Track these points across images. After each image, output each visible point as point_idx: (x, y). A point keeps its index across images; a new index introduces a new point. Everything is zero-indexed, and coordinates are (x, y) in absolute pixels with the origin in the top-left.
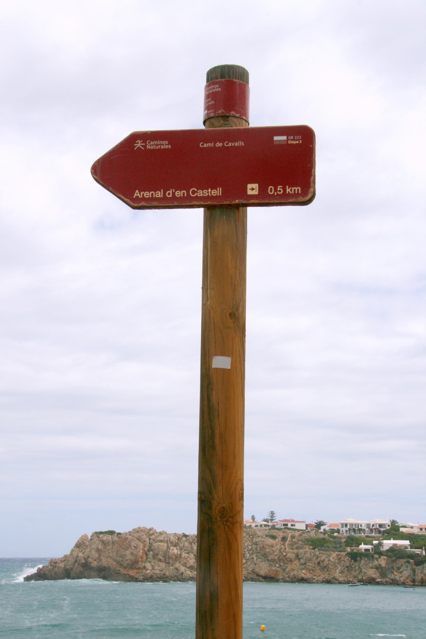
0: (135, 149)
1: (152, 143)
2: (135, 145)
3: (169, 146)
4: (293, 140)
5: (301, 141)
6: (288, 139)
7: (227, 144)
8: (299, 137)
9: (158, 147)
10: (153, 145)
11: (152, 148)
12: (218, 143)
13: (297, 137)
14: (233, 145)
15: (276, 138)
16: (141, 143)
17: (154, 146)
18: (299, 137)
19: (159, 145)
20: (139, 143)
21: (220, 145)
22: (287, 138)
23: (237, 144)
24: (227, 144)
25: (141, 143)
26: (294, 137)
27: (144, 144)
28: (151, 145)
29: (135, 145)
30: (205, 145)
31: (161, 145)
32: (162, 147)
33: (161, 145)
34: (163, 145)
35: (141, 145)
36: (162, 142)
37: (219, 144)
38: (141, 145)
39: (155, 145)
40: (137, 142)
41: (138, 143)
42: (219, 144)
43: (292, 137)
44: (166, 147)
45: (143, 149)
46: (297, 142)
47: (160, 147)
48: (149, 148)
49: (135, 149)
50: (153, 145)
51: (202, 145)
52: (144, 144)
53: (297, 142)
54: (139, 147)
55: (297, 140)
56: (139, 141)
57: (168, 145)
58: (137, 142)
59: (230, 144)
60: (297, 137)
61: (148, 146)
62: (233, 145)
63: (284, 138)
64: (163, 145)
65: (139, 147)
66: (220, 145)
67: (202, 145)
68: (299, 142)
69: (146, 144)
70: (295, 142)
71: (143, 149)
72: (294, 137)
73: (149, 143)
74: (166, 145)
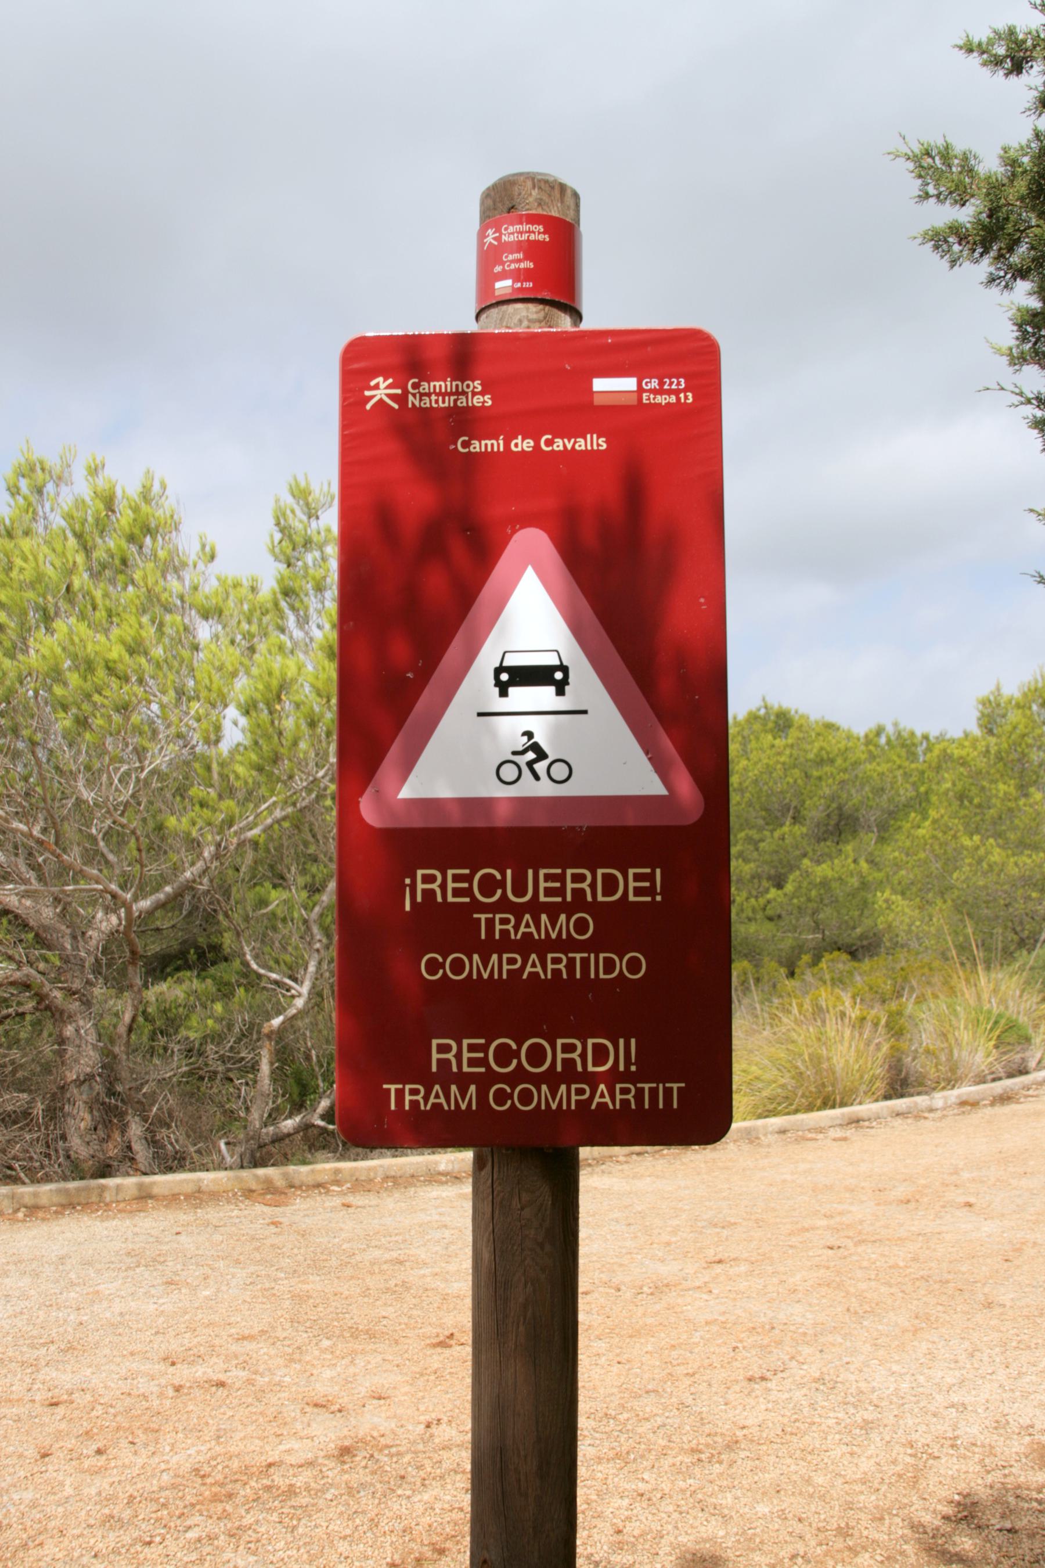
2: (367, 393)
14: (569, 447)
16: (387, 387)
17: (434, 397)
20: (382, 386)
23: (581, 445)
29: (367, 393)
38: (388, 395)
40: (373, 383)
41: (377, 387)
47: (455, 401)
48: (417, 403)
54: (381, 400)
58: (373, 383)
59: (559, 445)
61: (411, 398)
62: (569, 447)
65: (381, 400)
69: (406, 393)
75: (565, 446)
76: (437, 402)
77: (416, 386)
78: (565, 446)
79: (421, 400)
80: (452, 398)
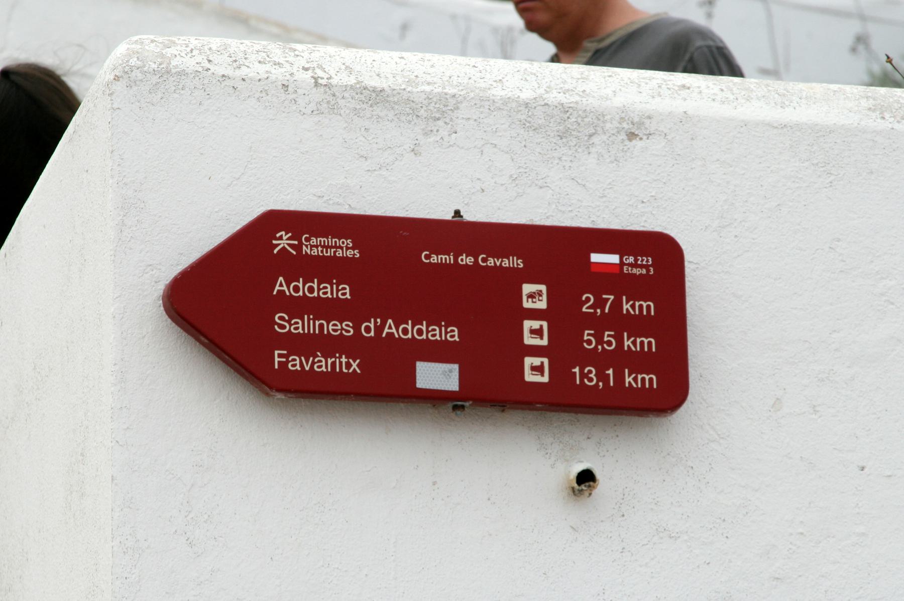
0: (275, 251)
1: (314, 241)
2: (274, 242)
3: (356, 251)
4: (635, 265)
5: (652, 269)
6: (622, 264)
7: (484, 260)
8: (647, 261)
9: (330, 253)
10: (317, 246)
11: (315, 252)
12: (464, 257)
13: (642, 260)
14: (498, 264)
15: (596, 258)
16: (288, 239)
17: (320, 249)
18: (647, 261)
19: (332, 247)
20: (285, 238)
21: (470, 260)
22: (621, 259)
23: (506, 263)
24: (484, 260)
25: (288, 239)
26: (636, 260)
27: (296, 242)
28: (312, 246)
29: (274, 242)
30: (434, 259)
31: (336, 247)
32: (339, 253)
33: (336, 247)
34: (342, 248)
35: (288, 244)
36: (339, 242)
37: (466, 260)
38: (289, 245)
39: (323, 247)
40: (278, 235)
41: (281, 238)
42: (466, 260)
43: (631, 259)
44: (350, 253)
45: (294, 253)
46: (644, 271)
47: (335, 252)
48: (309, 252)
49: (275, 251)
50: (317, 246)
51: (427, 257)
52: (296, 242)
53: (644, 271)
54: (284, 247)
55: (642, 266)
56: (283, 233)
57: (353, 248)
58: (278, 235)
59: (491, 262)
60: (642, 260)
61: (304, 248)
62: (498, 264)
63: (614, 259)
64: (342, 248)
65: (284, 247)
66: (470, 260)
67: (427, 257)
68: (648, 271)
69: (301, 244)
70: (637, 271)
71: (294, 253)
72: (636, 260)
73: (307, 240)
74: (347, 248)
75: (495, 263)
76: (322, 252)
77: (307, 240)
78: (495, 263)
79: (311, 250)
80: (333, 250)
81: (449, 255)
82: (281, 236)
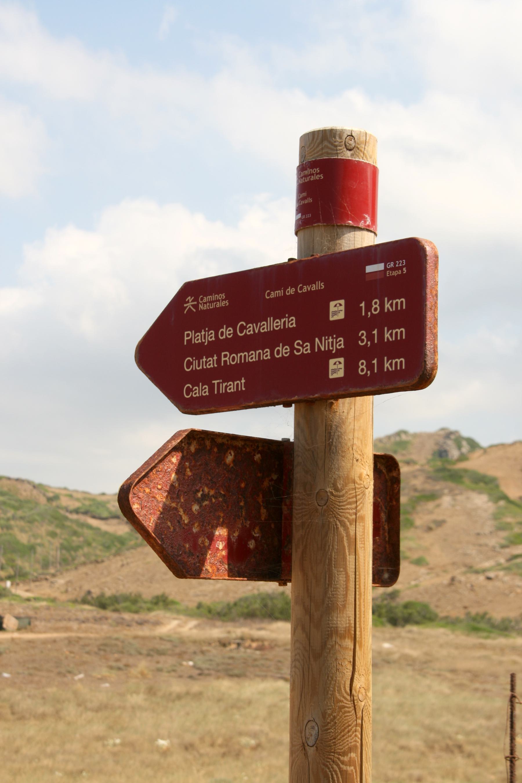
5: (404, 269)
6: (386, 269)
12: (289, 289)
20: (190, 301)
24: (301, 289)
30: (273, 295)
35: (192, 305)
37: (291, 291)
38: (192, 305)
40: (187, 300)
41: (188, 302)
42: (291, 291)
43: (392, 265)
51: (269, 294)
58: (187, 300)
63: (380, 267)
65: (190, 308)
68: (402, 271)
81: (281, 290)
82: (189, 300)
